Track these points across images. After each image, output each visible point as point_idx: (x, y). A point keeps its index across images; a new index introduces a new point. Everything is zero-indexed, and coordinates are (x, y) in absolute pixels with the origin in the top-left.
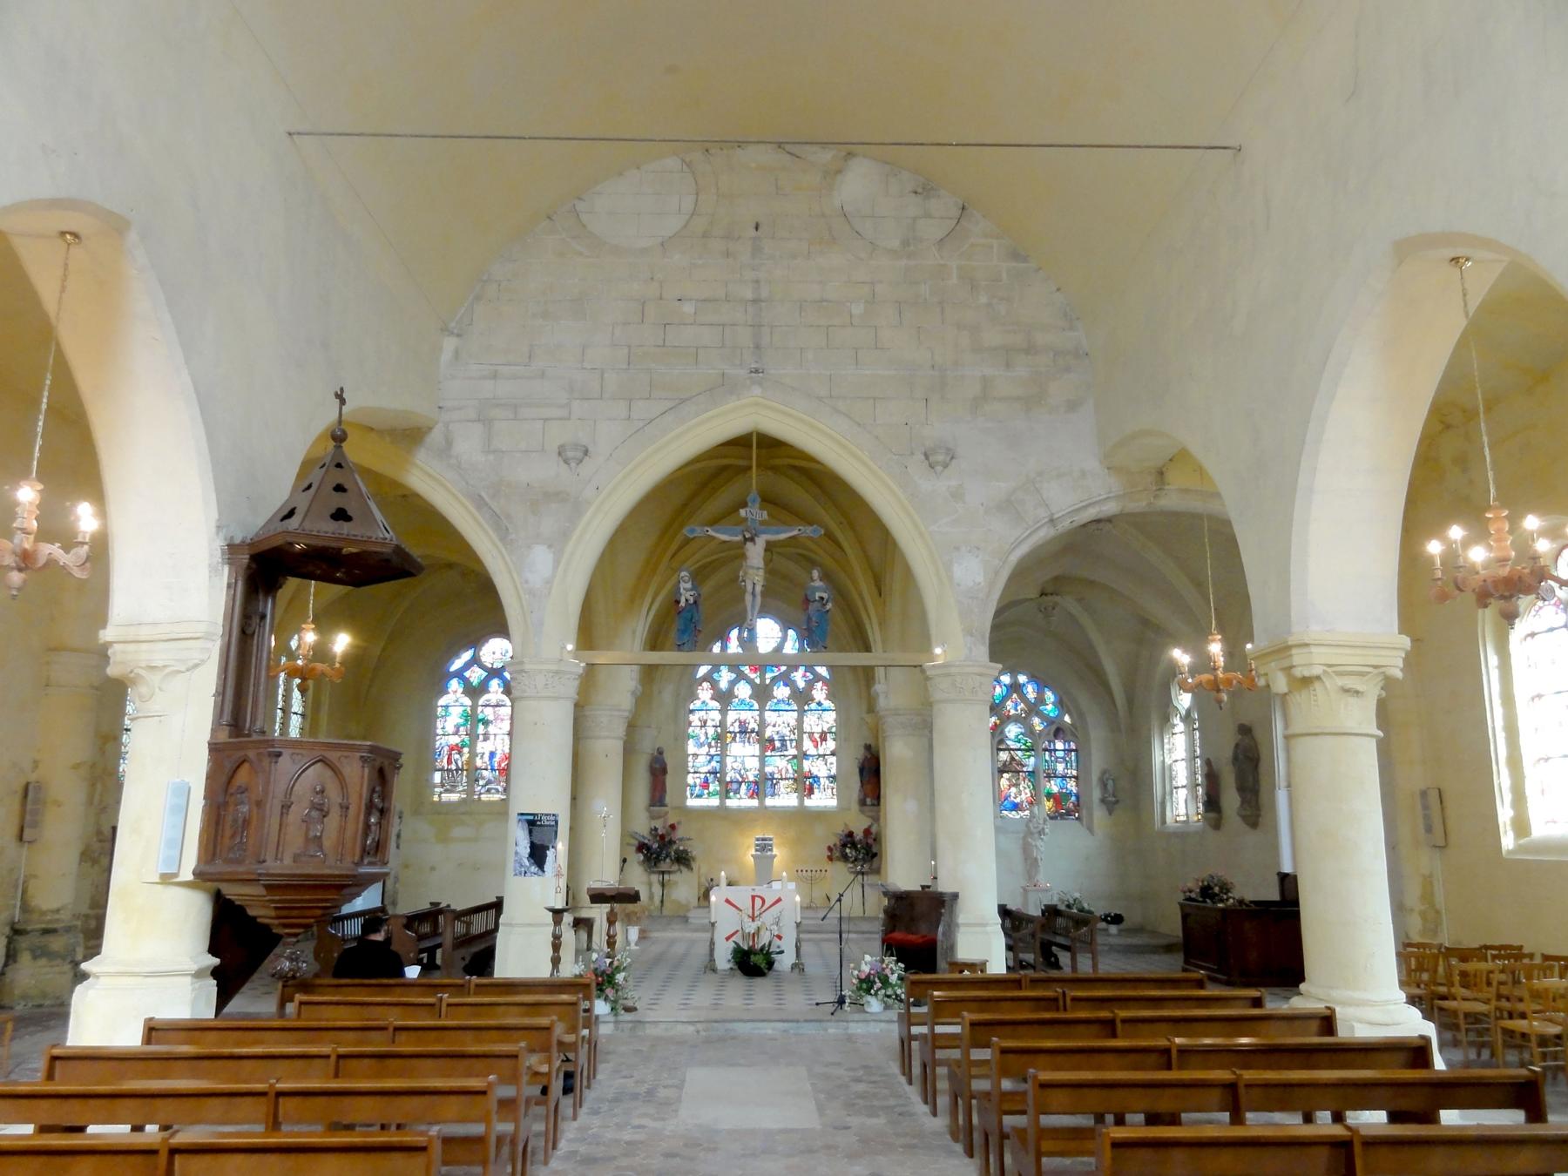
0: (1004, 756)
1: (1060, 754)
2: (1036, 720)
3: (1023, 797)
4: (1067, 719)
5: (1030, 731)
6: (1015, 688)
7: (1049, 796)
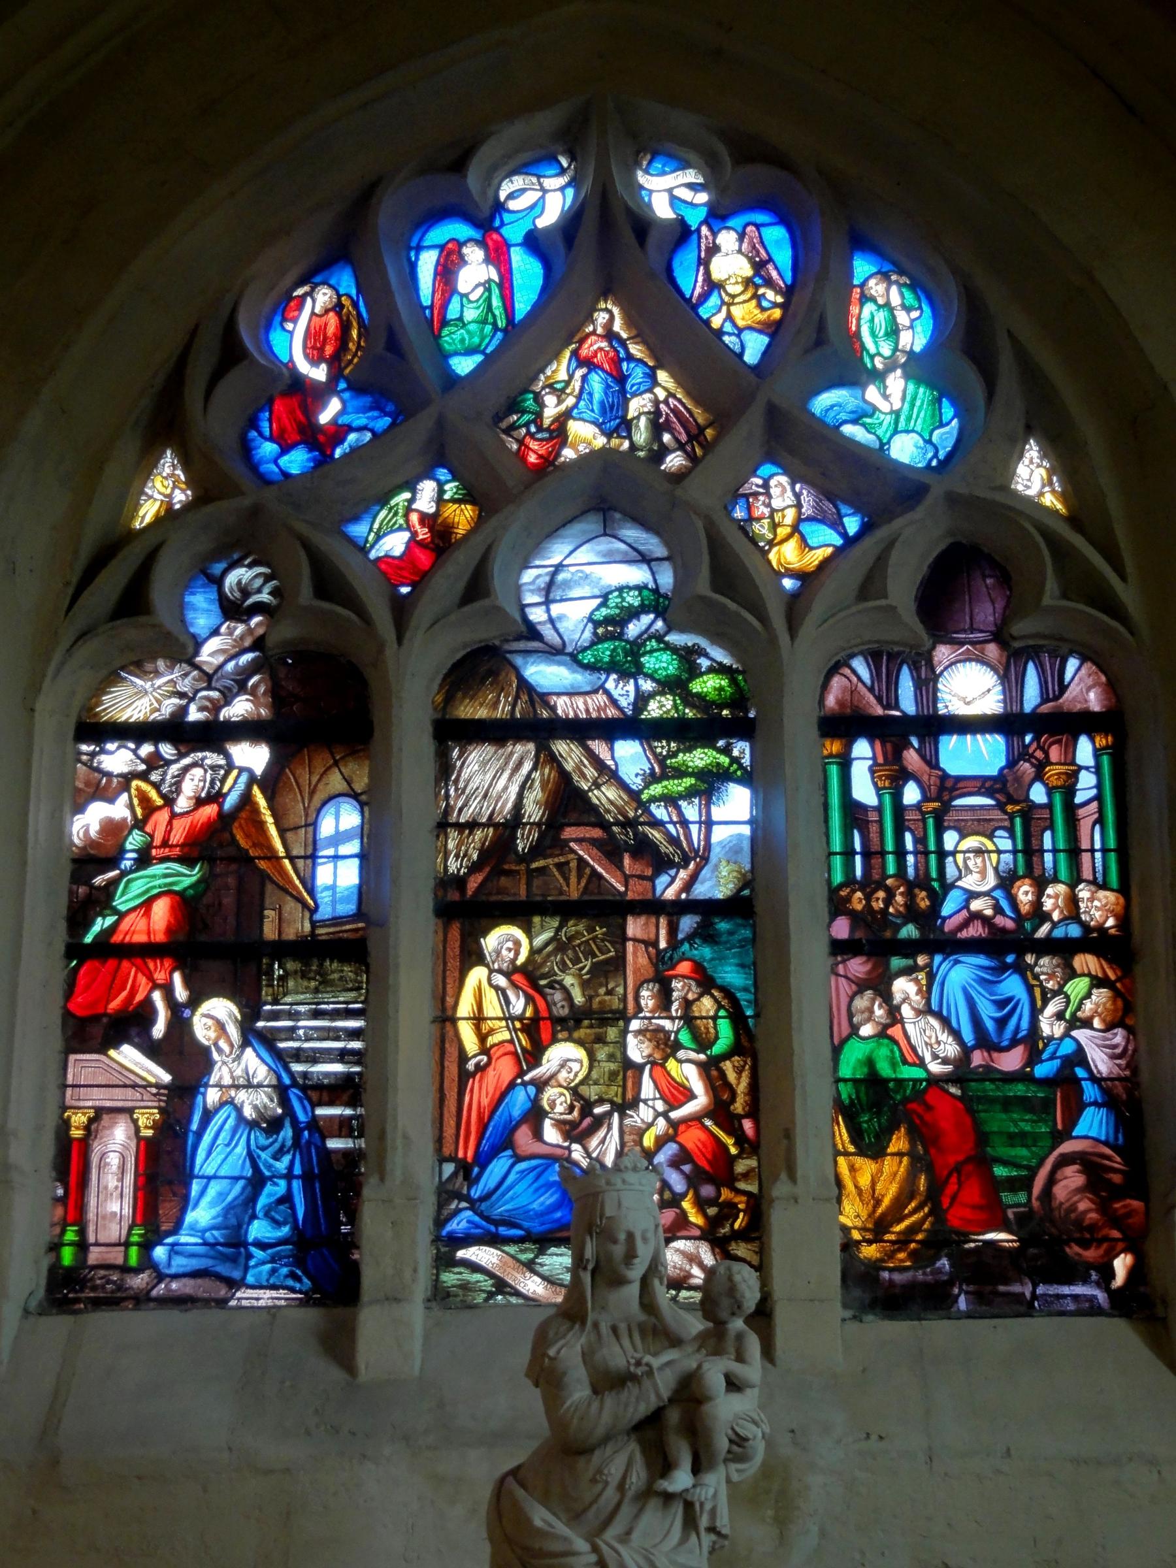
0: (495, 782)
1: (974, 756)
2: (779, 495)
3: (648, 1113)
4: (1033, 476)
5: (717, 581)
6: (610, 250)
7: (878, 1107)
